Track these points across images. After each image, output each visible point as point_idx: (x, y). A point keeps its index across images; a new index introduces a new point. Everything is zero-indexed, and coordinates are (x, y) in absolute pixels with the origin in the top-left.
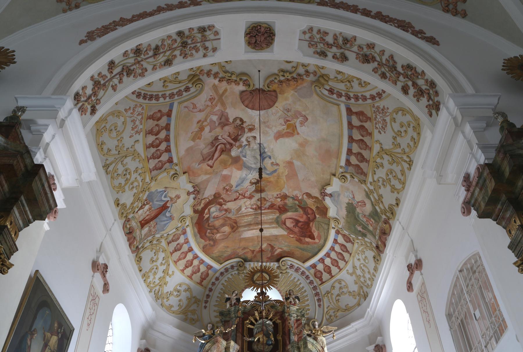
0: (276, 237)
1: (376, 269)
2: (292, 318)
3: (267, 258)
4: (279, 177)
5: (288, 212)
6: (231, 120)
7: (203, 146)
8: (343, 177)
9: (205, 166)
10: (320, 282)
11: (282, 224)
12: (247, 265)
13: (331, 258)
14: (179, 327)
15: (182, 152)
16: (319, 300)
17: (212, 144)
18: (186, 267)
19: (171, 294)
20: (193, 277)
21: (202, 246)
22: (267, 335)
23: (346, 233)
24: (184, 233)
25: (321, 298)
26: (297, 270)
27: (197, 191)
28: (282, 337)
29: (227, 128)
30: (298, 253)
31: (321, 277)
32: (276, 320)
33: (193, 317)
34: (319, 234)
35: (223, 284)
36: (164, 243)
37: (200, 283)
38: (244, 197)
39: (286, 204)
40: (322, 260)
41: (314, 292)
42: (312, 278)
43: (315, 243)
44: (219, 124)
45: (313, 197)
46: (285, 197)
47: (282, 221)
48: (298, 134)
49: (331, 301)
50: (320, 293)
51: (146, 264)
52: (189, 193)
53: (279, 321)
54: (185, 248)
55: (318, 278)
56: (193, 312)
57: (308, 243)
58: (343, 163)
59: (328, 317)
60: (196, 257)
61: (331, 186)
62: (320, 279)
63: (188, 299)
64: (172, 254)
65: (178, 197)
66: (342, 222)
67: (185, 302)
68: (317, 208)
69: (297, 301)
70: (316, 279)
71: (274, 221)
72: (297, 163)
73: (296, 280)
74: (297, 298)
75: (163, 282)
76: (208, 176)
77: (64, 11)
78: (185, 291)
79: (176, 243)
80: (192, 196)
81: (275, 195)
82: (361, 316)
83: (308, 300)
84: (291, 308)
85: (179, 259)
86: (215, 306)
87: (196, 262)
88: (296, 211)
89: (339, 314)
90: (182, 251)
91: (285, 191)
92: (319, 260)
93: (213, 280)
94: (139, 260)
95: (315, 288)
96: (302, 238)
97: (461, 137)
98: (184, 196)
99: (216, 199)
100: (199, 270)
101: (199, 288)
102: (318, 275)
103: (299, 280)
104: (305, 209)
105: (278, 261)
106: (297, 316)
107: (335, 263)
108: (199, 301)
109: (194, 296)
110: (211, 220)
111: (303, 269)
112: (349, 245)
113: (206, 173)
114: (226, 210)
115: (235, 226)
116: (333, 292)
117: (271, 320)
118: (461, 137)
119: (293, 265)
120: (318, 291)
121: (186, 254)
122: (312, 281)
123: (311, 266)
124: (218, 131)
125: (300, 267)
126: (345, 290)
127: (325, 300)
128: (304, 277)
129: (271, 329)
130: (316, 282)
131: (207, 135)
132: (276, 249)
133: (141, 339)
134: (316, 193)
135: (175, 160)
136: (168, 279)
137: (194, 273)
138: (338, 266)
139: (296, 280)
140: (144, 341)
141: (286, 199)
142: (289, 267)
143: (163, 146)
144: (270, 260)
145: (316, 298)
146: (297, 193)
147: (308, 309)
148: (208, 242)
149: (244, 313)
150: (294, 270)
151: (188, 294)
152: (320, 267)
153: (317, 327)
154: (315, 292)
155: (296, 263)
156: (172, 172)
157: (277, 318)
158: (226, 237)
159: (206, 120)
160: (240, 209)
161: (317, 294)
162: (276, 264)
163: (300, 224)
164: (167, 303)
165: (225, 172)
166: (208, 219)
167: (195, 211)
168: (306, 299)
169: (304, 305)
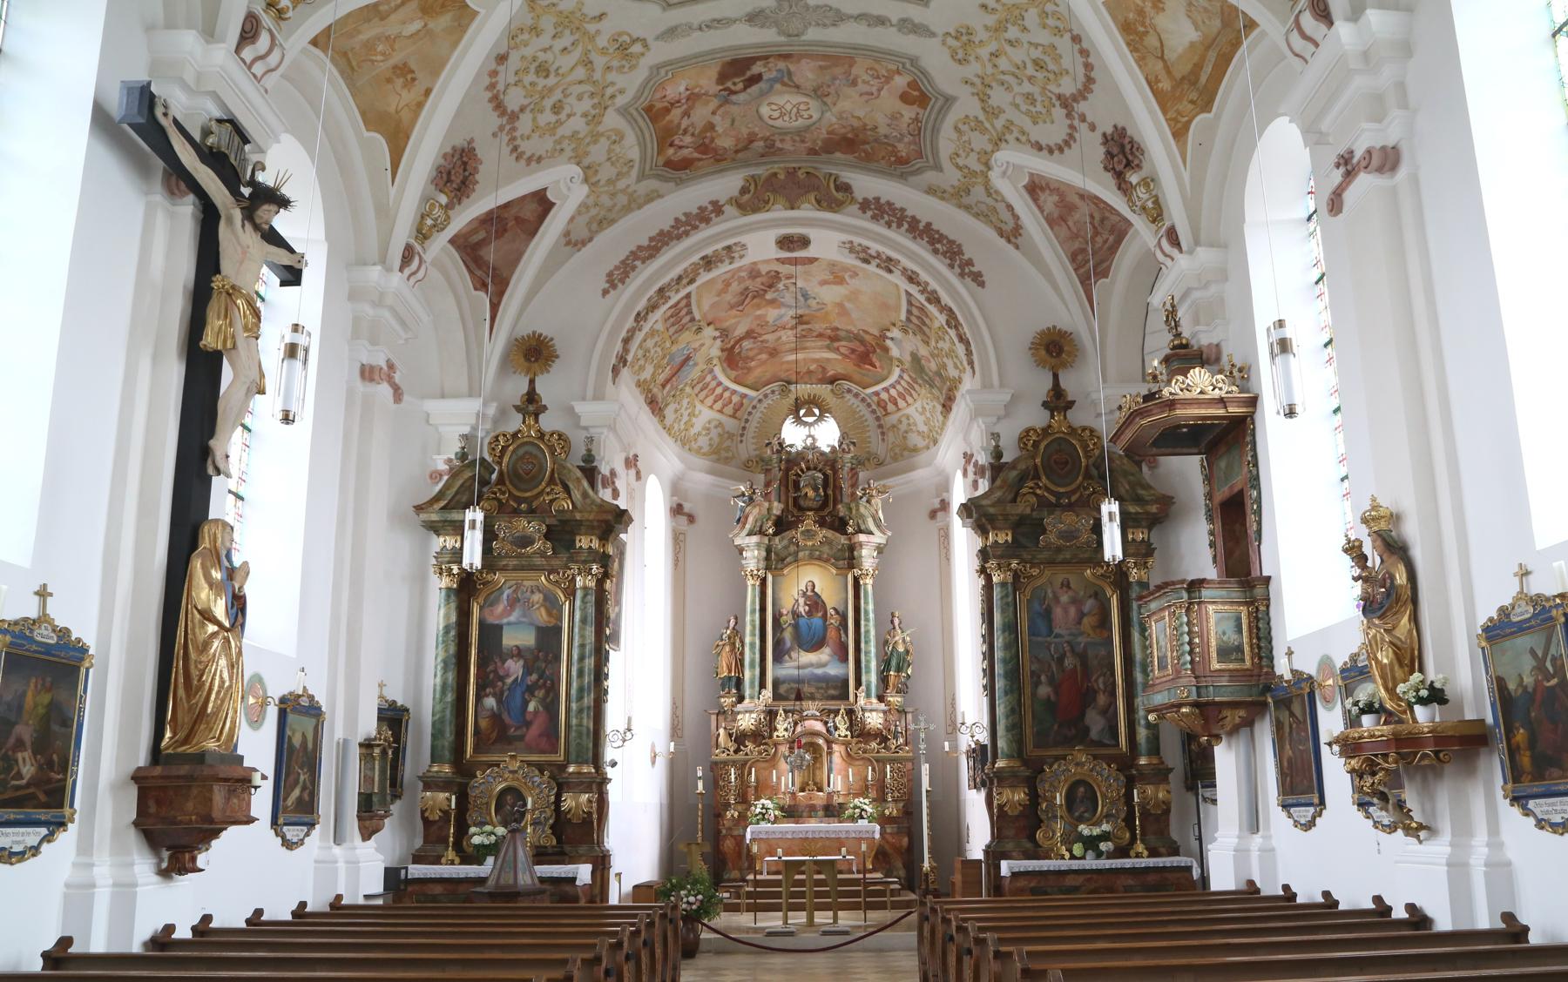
0: (828, 360)
1: (944, 424)
4: (827, 313)
6: (764, 273)
7: (729, 297)
8: (905, 331)
9: (734, 312)
12: (792, 387)
14: (711, 472)
15: (706, 306)
17: (742, 294)
18: (715, 402)
19: (699, 434)
20: (725, 410)
21: (733, 377)
22: (816, 489)
23: (913, 376)
24: (711, 371)
25: (885, 430)
26: (856, 395)
27: (724, 334)
29: (759, 280)
30: (857, 377)
33: (726, 455)
35: (762, 412)
36: (688, 389)
37: (733, 416)
38: (784, 328)
40: (886, 390)
42: (874, 407)
44: (749, 278)
45: (871, 335)
46: (837, 329)
51: (668, 422)
52: (715, 338)
54: (714, 384)
56: (728, 449)
57: (869, 370)
58: (903, 316)
60: (726, 389)
62: (885, 409)
63: (720, 435)
64: (697, 395)
65: (702, 345)
66: (907, 365)
67: (717, 440)
68: (877, 343)
69: (852, 448)
72: (848, 305)
74: (854, 443)
75: (689, 425)
76: (736, 320)
77: (579, 250)
78: (716, 427)
79: (701, 385)
80: (718, 342)
82: (929, 464)
85: (707, 396)
86: (753, 438)
87: (727, 394)
88: (851, 341)
89: (906, 453)
90: (709, 387)
91: (836, 324)
93: (750, 409)
94: (662, 418)
97: (975, 425)
98: (708, 342)
99: (749, 334)
100: (730, 402)
101: (732, 421)
102: (882, 405)
104: (862, 342)
105: (832, 382)
107: (900, 395)
108: (734, 435)
109: (727, 429)
110: (744, 352)
112: (915, 386)
113: (736, 317)
114: (762, 342)
115: (774, 353)
116: (900, 426)
117: (820, 471)
118: (975, 425)
120: (882, 422)
121: (714, 390)
124: (748, 283)
126: (914, 428)
127: (891, 434)
129: (820, 481)
130: (880, 412)
131: (735, 287)
133: (672, 495)
135: (698, 317)
136: (694, 420)
137: (725, 406)
138: (904, 399)
140: (675, 498)
143: (684, 312)
144: (822, 381)
145: (879, 431)
147: (870, 442)
148: (740, 372)
149: (788, 461)
151: (720, 430)
152: (884, 396)
156: (694, 328)
158: (763, 363)
159: (733, 277)
160: (780, 338)
161: (880, 426)
162: (830, 387)
164: (695, 446)
165: (759, 312)
166: (739, 353)
167: (723, 350)
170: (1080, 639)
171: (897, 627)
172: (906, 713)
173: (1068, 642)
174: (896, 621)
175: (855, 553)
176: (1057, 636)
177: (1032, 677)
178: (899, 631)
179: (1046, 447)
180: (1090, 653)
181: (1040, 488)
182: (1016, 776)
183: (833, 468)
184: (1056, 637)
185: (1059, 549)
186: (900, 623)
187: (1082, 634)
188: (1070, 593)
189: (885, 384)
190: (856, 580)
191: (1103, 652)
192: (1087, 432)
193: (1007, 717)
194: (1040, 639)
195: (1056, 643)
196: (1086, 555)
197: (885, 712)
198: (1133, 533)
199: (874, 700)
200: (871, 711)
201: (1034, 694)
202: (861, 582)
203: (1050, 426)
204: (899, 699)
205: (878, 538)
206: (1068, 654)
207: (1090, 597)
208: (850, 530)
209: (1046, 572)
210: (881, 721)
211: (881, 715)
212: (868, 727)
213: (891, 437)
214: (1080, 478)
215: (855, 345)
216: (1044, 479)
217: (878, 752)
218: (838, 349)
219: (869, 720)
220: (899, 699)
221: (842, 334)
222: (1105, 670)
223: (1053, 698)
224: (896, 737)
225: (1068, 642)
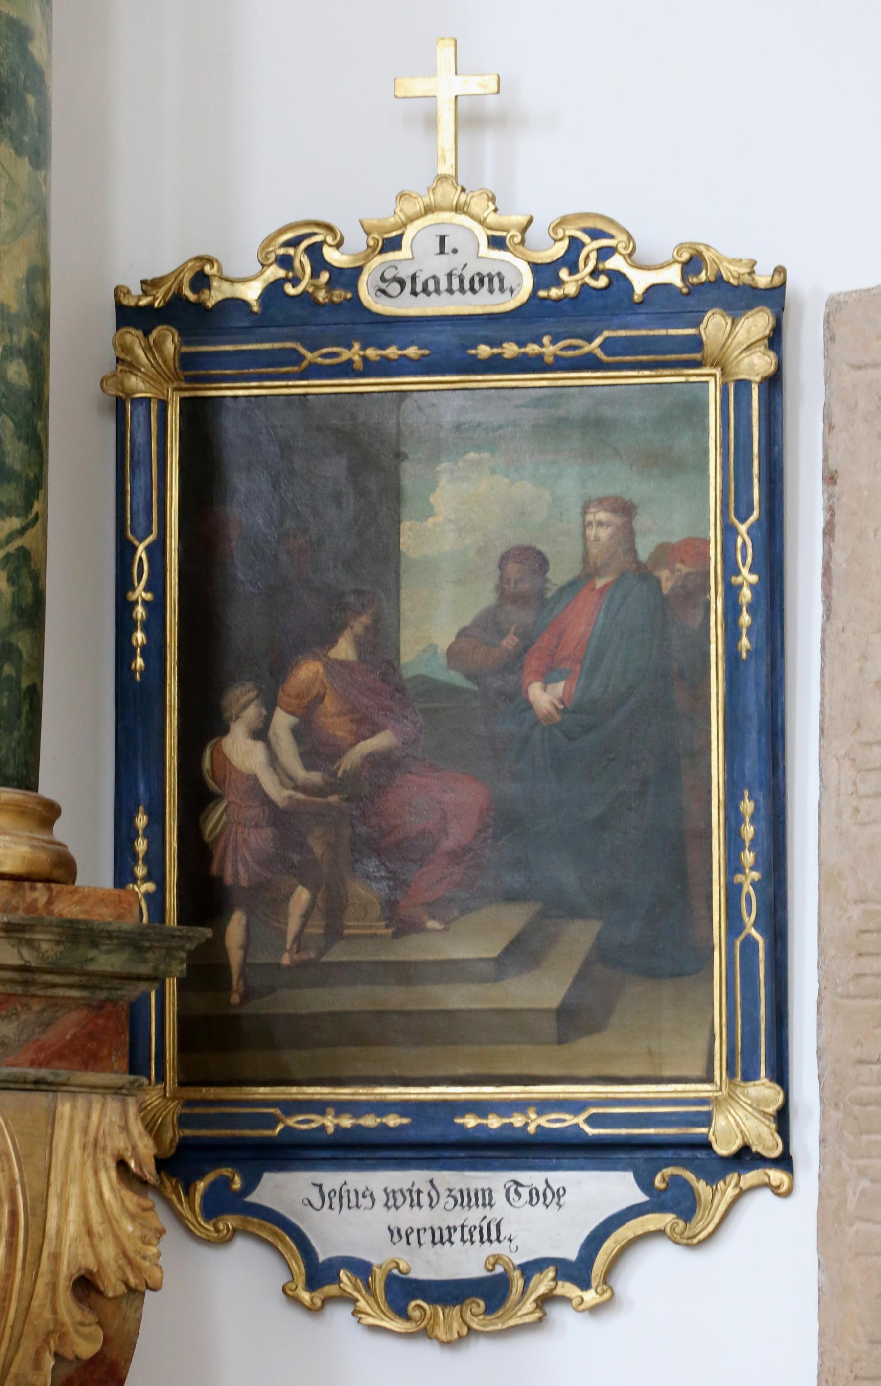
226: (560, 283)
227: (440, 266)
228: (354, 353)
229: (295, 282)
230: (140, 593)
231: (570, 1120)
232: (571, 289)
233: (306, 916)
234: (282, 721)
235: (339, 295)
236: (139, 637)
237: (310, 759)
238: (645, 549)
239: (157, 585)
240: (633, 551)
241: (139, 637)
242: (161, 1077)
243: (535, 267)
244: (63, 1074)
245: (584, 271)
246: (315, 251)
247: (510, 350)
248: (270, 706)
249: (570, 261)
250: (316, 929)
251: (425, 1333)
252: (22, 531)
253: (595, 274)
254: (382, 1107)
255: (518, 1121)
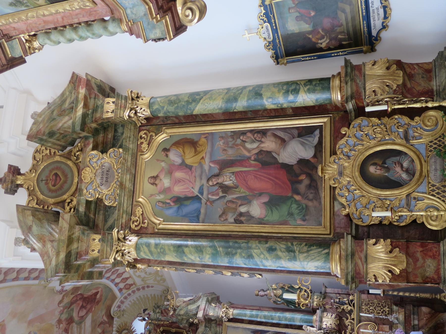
0: (93, 321)
2: (160, 317)
3: (110, 327)
5: (73, 316)
10: (134, 286)
11: (82, 318)
13: (116, 278)
16: (148, 287)
28: (173, 328)
31: (130, 285)
32: (160, 331)
34: (95, 289)
39: (66, 319)
40: (116, 285)
41: (141, 290)
42: (130, 292)
43: (102, 291)
45: (63, 298)
46: (59, 321)
47: (80, 319)
48: (4, 321)
49: (149, 278)
50: (143, 286)
53: (161, 329)
55: (130, 287)
57: (101, 296)
58: (36, 282)
59: (161, 282)
61: (55, 287)
68: (72, 294)
69: (146, 312)
70: (131, 288)
71: (79, 326)
72: (31, 317)
73: (130, 303)
74: (145, 310)
81: (57, 329)
83: (147, 295)
84: (152, 317)
91: (54, 321)
92: (116, 286)
95: (138, 289)
96: (96, 300)
103: (130, 301)
105: (113, 318)
106: (159, 312)
111: (122, 298)
116: (142, 276)
119: (118, 306)
120: (141, 287)
122: (132, 291)
123: (120, 292)
125: (120, 300)
128: (128, 297)
130: (134, 288)
132: (102, 320)
134: (59, 297)
139: (130, 303)
141: (61, 320)
142: (119, 309)
146: (57, 313)
147: (154, 295)
150: (122, 305)
152: (122, 285)
153: (168, 303)
154: (141, 289)
155: (116, 303)
157: (158, 330)
162: (115, 319)
163: (84, 305)
168: (146, 296)
169: (150, 298)
170: (206, 167)
171: (266, 293)
172: (326, 293)
173: (208, 180)
174: (262, 293)
175: (213, 318)
176: (201, 191)
177: (241, 222)
178: (268, 292)
179: (42, 193)
180: (221, 156)
181: (72, 200)
182: (353, 255)
183: (158, 326)
184: (202, 194)
185: (122, 186)
186: (263, 290)
187: (201, 165)
188: (162, 176)
189: (112, 286)
190: (230, 320)
191: (220, 143)
192: (36, 155)
193: (278, 258)
194: (203, 211)
195: (208, 194)
196: (129, 159)
197: (325, 310)
198: (108, 112)
199: (315, 317)
200: (321, 321)
201: (261, 222)
202: (231, 317)
203: (28, 189)
204: (316, 297)
205: (202, 303)
206: (220, 181)
207: (167, 156)
208: (196, 321)
209: (140, 200)
210: (329, 315)
211: (325, 314)
212: (334, 326)
213: (150, 282)
214: (69, 163)
215: (76, 308)
216: (65, 197)
217: (353, 319)
218: (82, 317)
219: (328, 325)
220: (316, 297)
221: (64, 316)
222: (239, 141)
223: (265, 199)
224: (343, 304)
225: (208, 180)
226: (265, 20)
227: (266, 33)
228: (277, 41)
229: (271, 48)
230: (308, 58)
231: (363, 2)
232: (266, 19)
233: (342, 35)
234: (320, 41)
235: (272, 43)
236: (312, 58)
237: (324, 38)
238: (293, 5)
239: (306, 57)
240: (294, 7)
241: (312, 58)
242: (362, 48)
243: (264, 23)
244: (363, 73)
245: (264, 18)
246: (268, 46)
247: (274, 25)
248: (318, 43)
249: (263, 20)
250: (343, 34)
251: (390, 14)
252: (302, 85)
253: (264, 17)
254: (363, 24)
255: (364, 8)
